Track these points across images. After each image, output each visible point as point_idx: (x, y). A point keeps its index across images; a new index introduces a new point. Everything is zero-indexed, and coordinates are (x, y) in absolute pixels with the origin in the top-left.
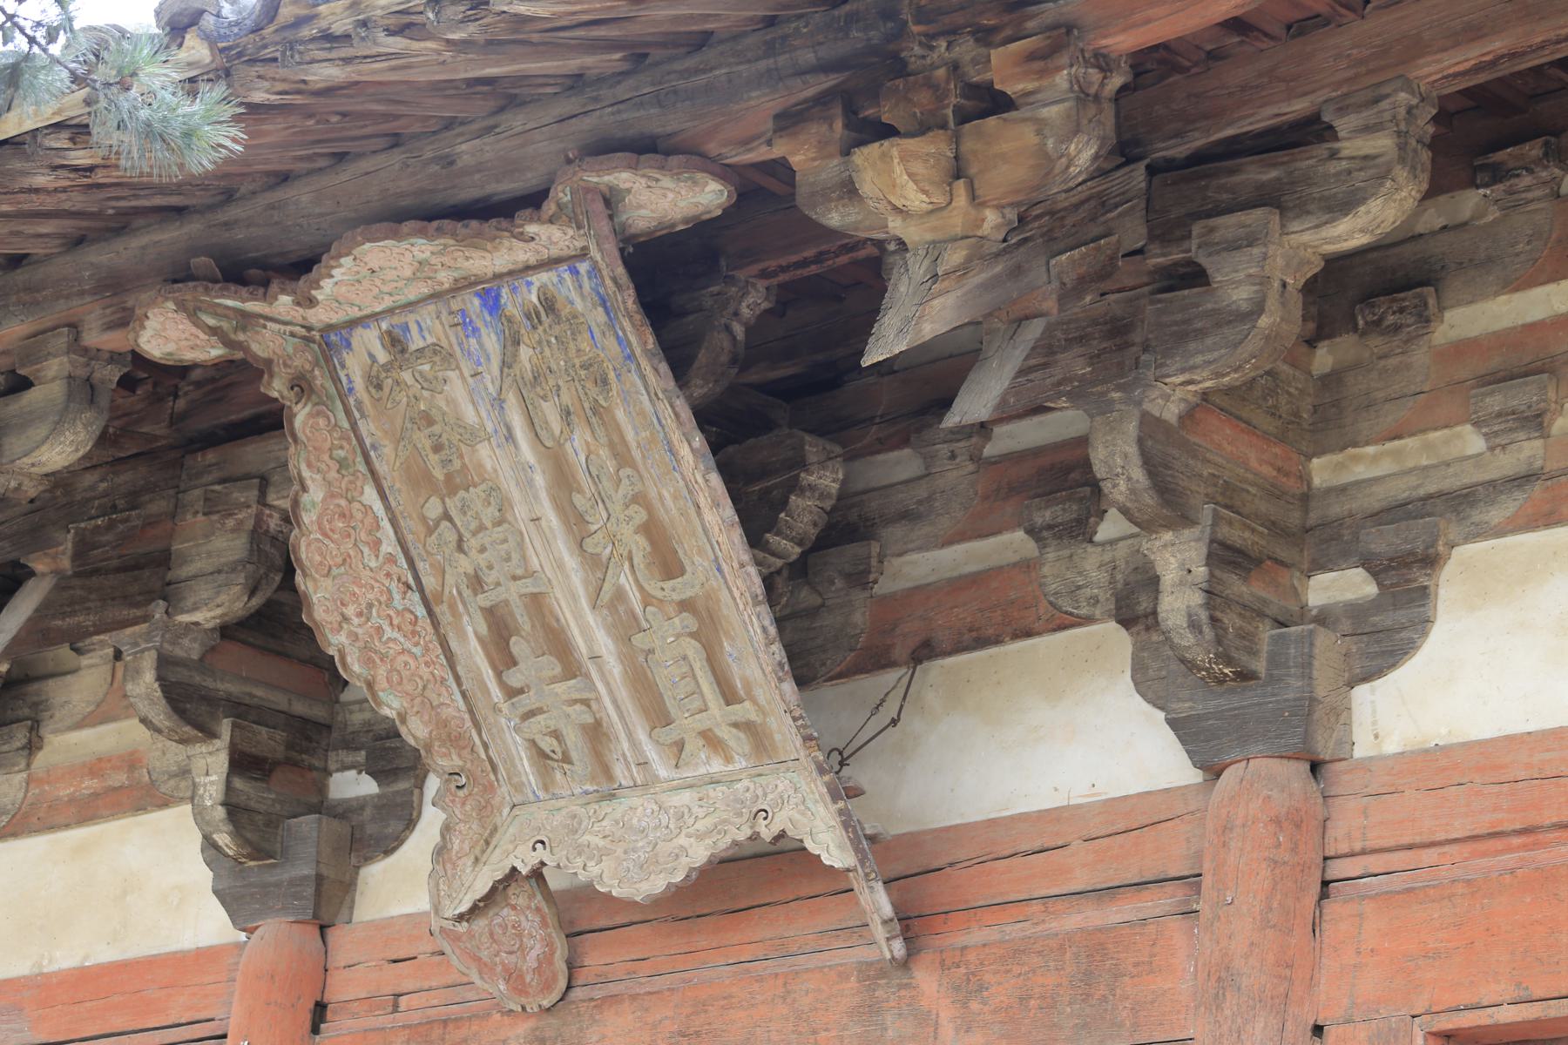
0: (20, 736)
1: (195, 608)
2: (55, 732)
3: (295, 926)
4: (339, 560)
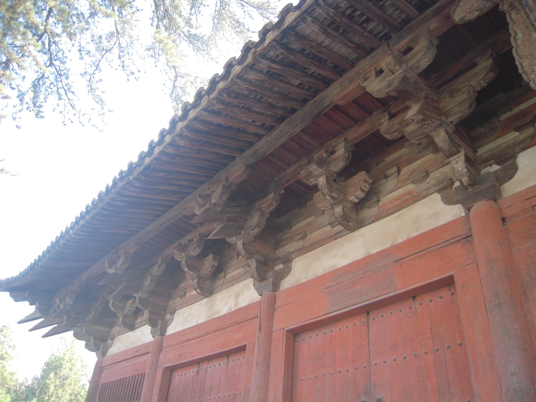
0: (375, 199)
1: (455, 114)
2: (384, 196)
3: (488, 201)
4: (529, 54)
